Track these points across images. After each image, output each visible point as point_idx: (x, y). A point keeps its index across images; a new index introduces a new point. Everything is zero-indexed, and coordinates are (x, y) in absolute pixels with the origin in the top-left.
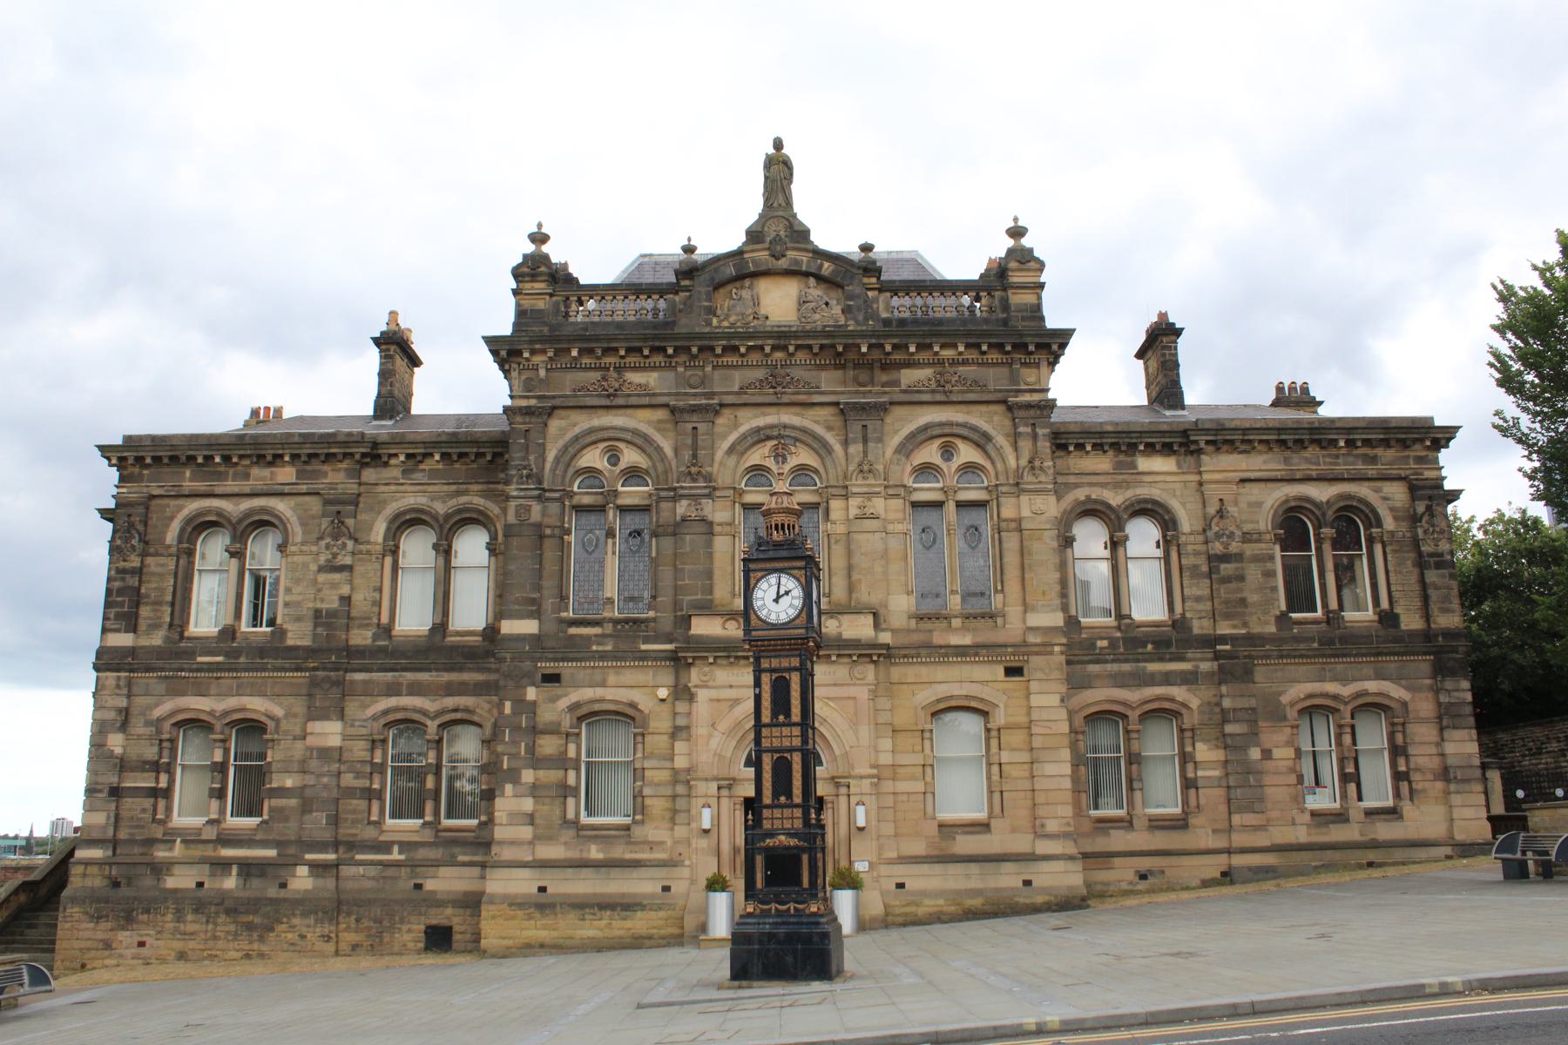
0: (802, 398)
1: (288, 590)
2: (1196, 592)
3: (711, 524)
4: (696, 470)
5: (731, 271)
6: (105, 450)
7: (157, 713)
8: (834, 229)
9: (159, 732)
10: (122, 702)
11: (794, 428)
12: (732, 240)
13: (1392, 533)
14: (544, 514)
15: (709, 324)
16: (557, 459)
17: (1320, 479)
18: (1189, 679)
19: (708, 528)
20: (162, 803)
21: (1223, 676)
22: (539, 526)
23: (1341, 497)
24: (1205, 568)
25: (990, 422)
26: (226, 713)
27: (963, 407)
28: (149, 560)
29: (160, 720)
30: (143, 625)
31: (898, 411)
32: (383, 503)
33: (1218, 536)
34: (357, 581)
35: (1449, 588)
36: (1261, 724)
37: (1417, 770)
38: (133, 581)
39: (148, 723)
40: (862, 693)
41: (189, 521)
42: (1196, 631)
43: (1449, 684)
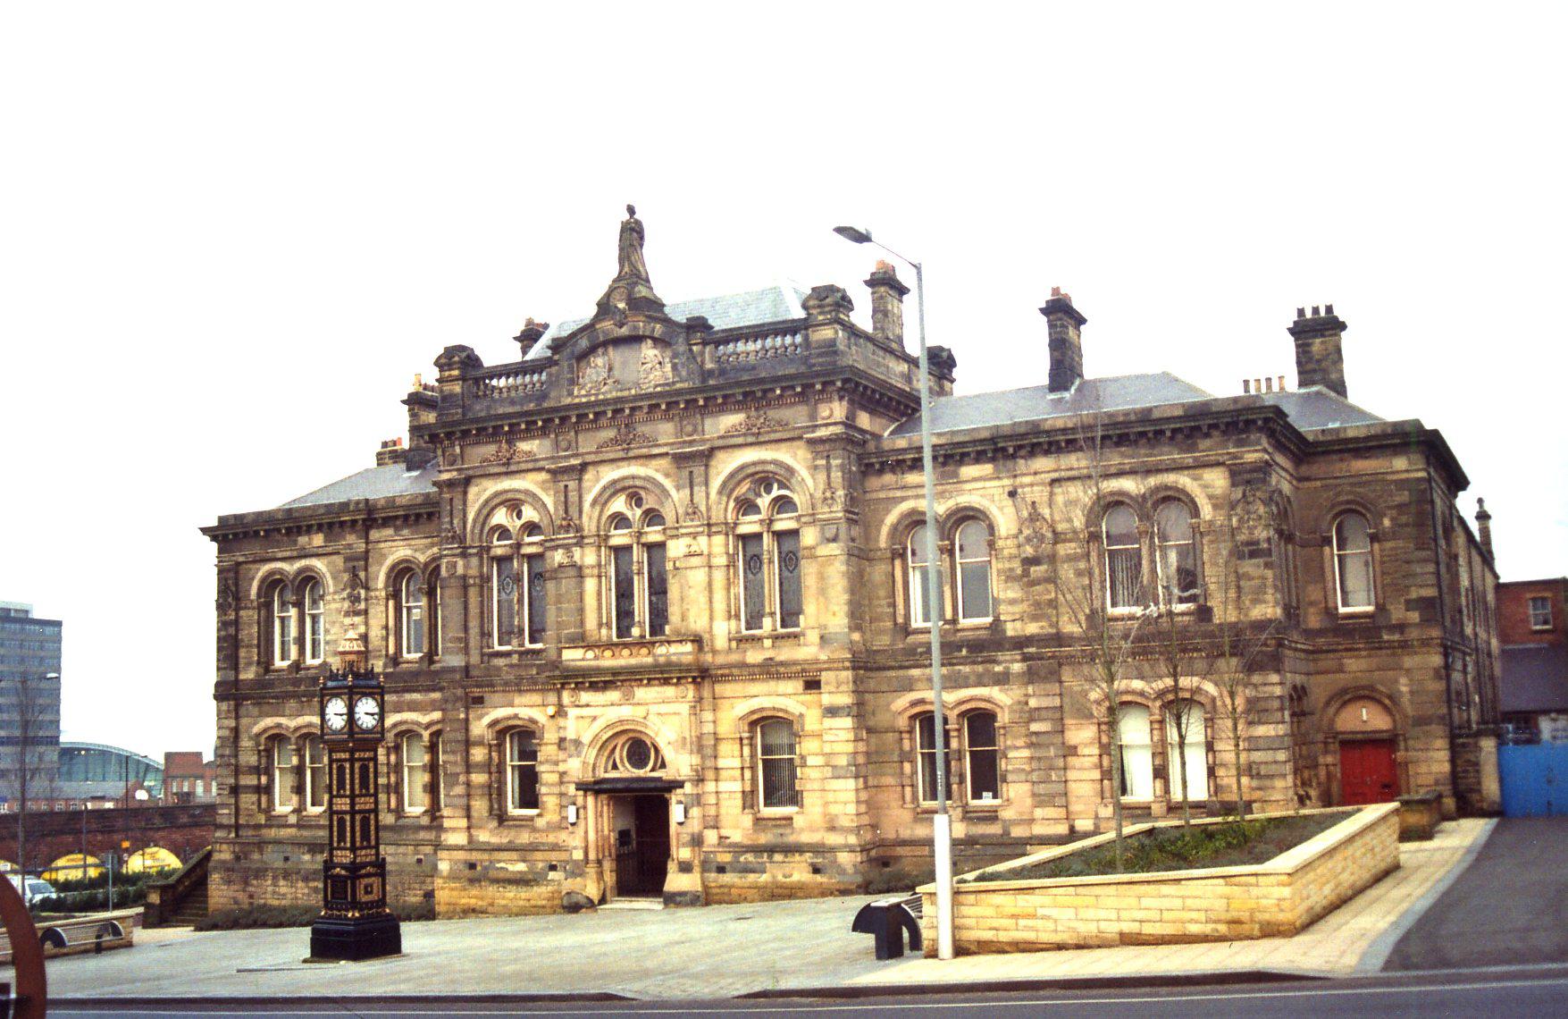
0: (644, 451)
1: (327, 631)
2: (1011, 594)
3: (580, 568)
4: (569, 524)
5: (584, 343)
6: (205, 531)
7: (256, 730)
8: (679, 287)
9: (258, 744)
10: (232, 723)
11: (639, 478)
12: (586, 312)
13: (1211, 523)
14: (466, 567)
15: (570, 394)
16: (475, 521)
17: (1132, 472)
18: (1002, 680)
19: (579, 572)
20: (264, 799)
21: (1031, 677)
22: (464, 577)
23: (1157, 489)
24: (1019, 571)
25: (795, 456)
26: (297, 729)
27: (773, 446)
28: (242, 613)
29: (259, 735)
30: (242, 662)
31: (721, 455)
32: (384, 556)
33: (1028, 540)
34: (372, 622)
35: (1264, 578)
36: (1068, 721)
37: (1222, 765)
38: (232, 631)
39: (250, 738)
40: (684, 708)
41: (263, 580)
42: (1010, 633)
43: (1256, 678)
